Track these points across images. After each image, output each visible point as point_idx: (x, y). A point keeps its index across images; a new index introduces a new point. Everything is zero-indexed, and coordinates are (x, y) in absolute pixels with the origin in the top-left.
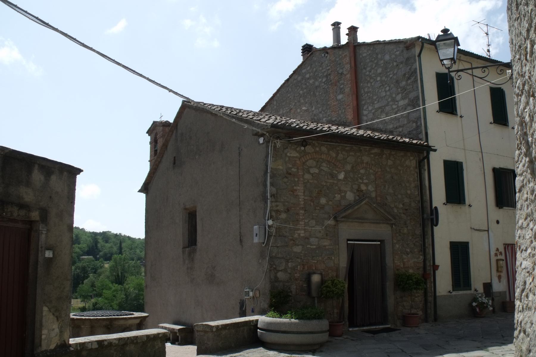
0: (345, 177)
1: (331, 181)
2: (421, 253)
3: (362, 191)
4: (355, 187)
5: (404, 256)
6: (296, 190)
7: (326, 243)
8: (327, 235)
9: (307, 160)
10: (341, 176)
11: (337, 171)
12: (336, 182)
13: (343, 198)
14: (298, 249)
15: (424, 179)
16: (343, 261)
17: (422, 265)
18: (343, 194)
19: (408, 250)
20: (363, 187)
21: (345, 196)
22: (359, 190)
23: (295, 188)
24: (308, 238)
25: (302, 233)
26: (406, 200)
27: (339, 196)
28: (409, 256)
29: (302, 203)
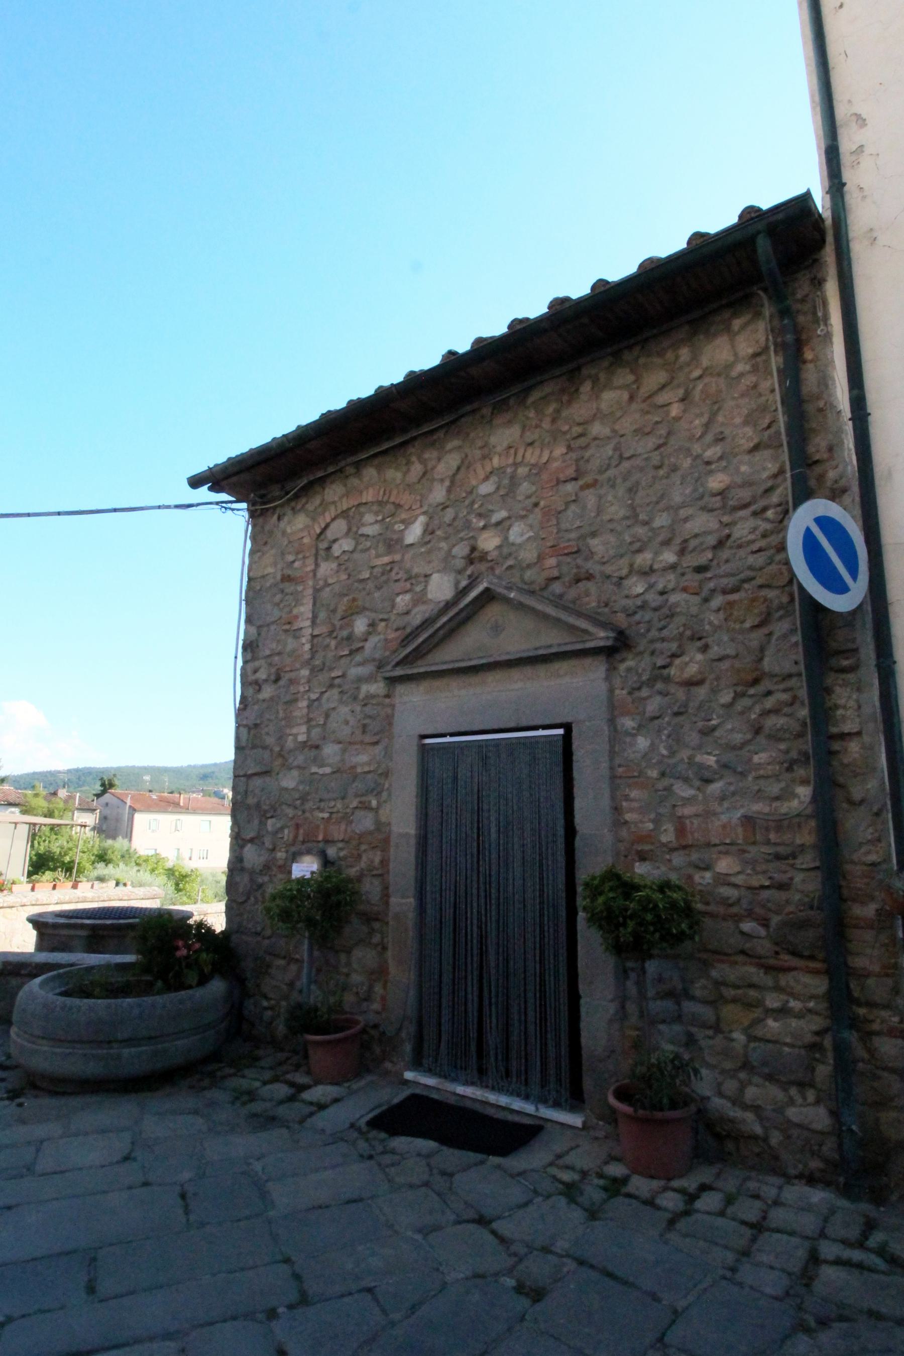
0: (428, 531)
1: (386, 559)
2: (801, 772)
3: (483, 557)
4: (461, 550)
5: (683, 791)
6: (296, 617)
7: (362, 759)
8: (364, 732)
9: (327, 526)
10: (414, 533)
11: (403, 522)
12: (397, 557)
13: (420, 599)
14: (289, 781)
15: (825, 381)
16: (401, 814)
17: (806, 837)
18: (418, 589)
19: (711, 760)
20: (489, 542)
21: (424, 591)
22: (475, 556)
23: (295, 611)
24: (317, 747)
25: (301, 733)
26: (702, 523)
27: (408, 597)
28: (716, 787)
29: (307, 647)
